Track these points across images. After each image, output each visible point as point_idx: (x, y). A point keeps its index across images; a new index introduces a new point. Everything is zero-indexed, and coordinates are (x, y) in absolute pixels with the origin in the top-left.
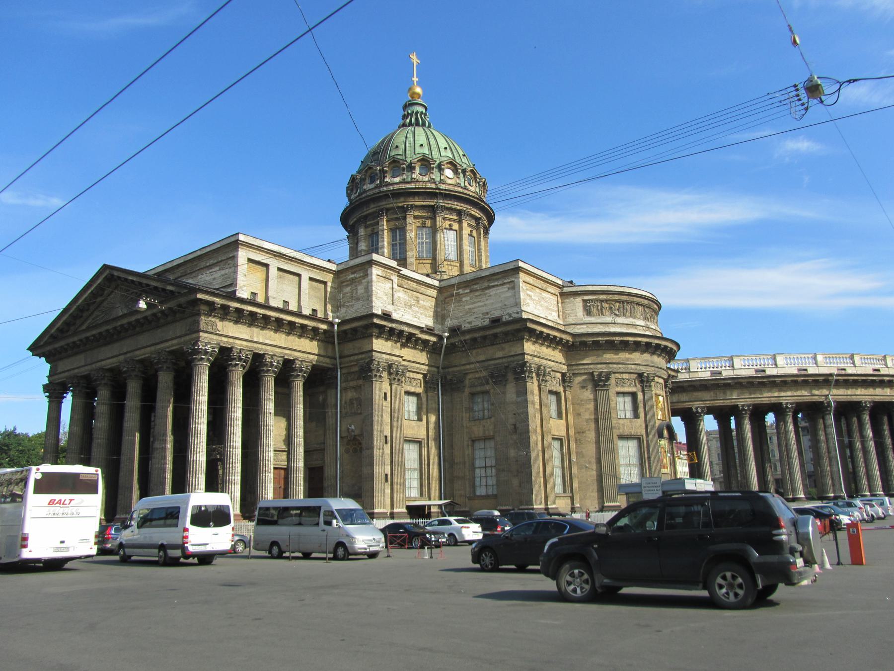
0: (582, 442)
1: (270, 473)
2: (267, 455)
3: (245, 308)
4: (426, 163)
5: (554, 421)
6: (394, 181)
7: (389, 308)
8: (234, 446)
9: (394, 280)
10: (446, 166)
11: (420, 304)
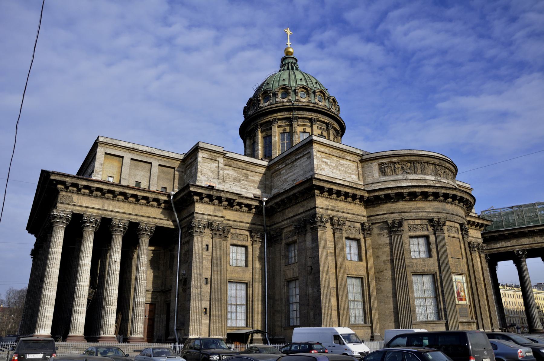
0: (380, 280)
1: (112, 305)
2: (110, 292)
3: (92, 185)
5: (352, 263)
6: (264, 105)
8: (81, 285)
9: (220, 161)
10: (300, 90)
11: (250, 179)
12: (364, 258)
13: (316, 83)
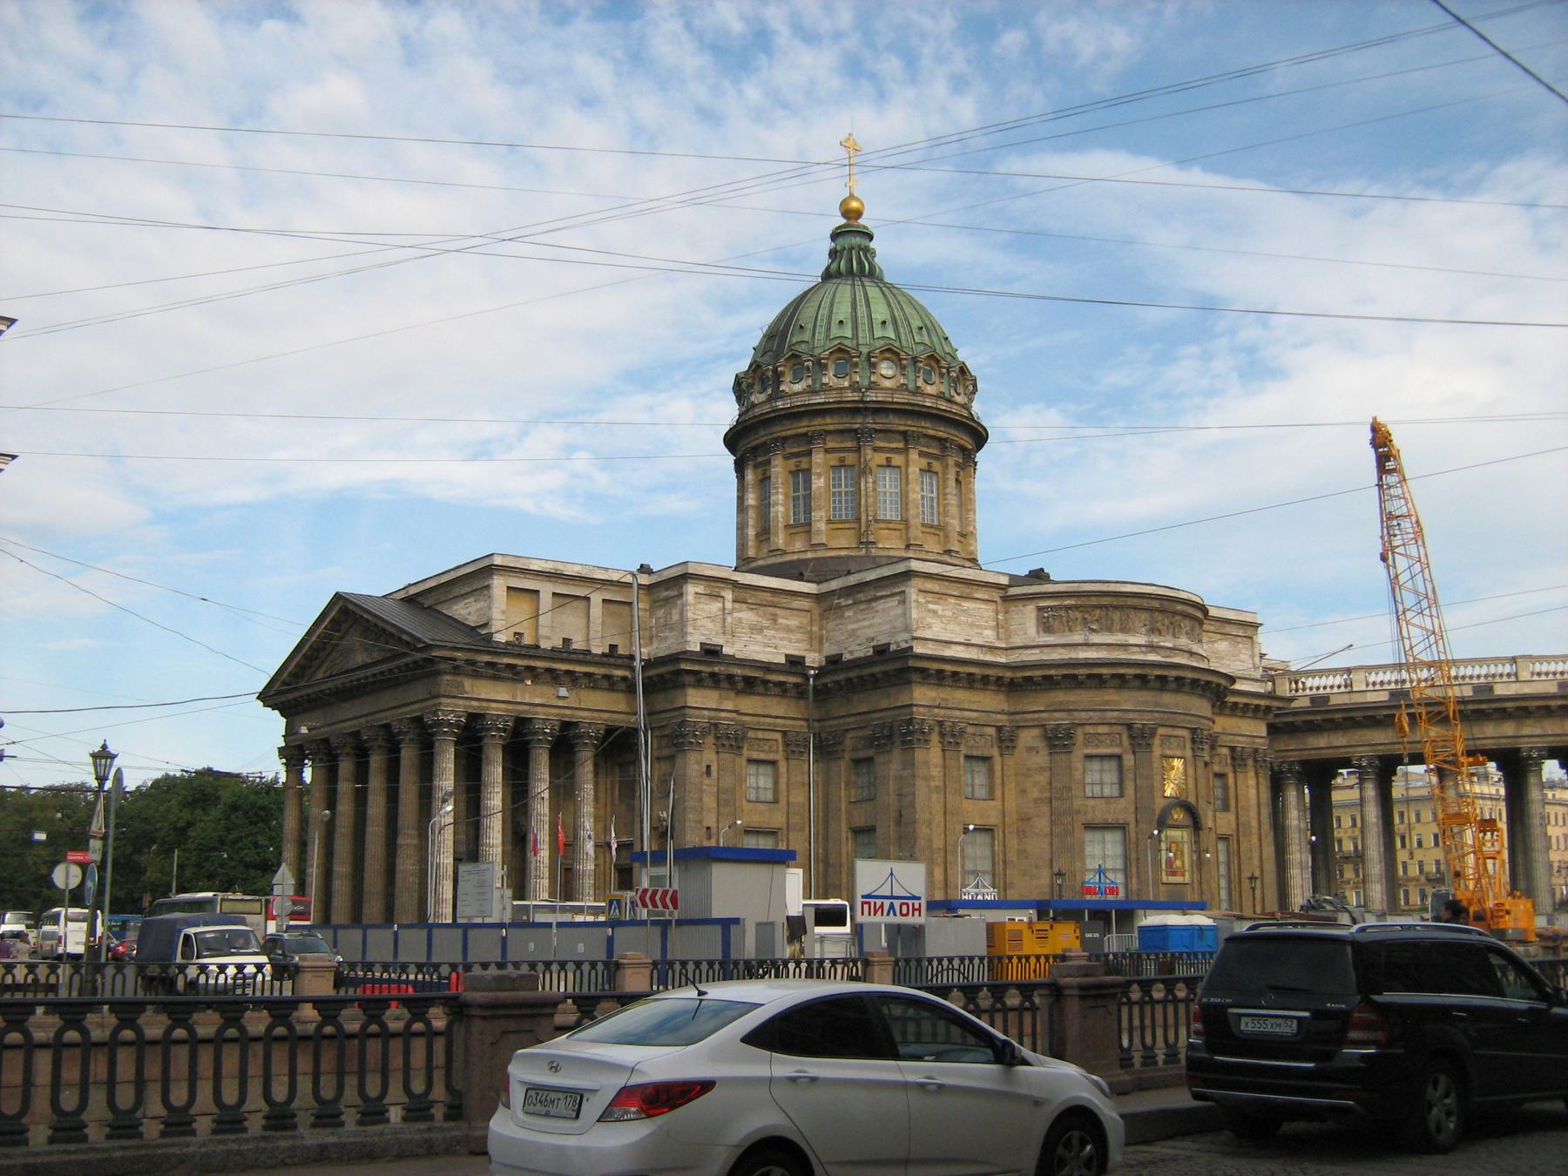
3: (500, 661)
4: (846, 356)
7: (717, 640)
12: (998, 793)
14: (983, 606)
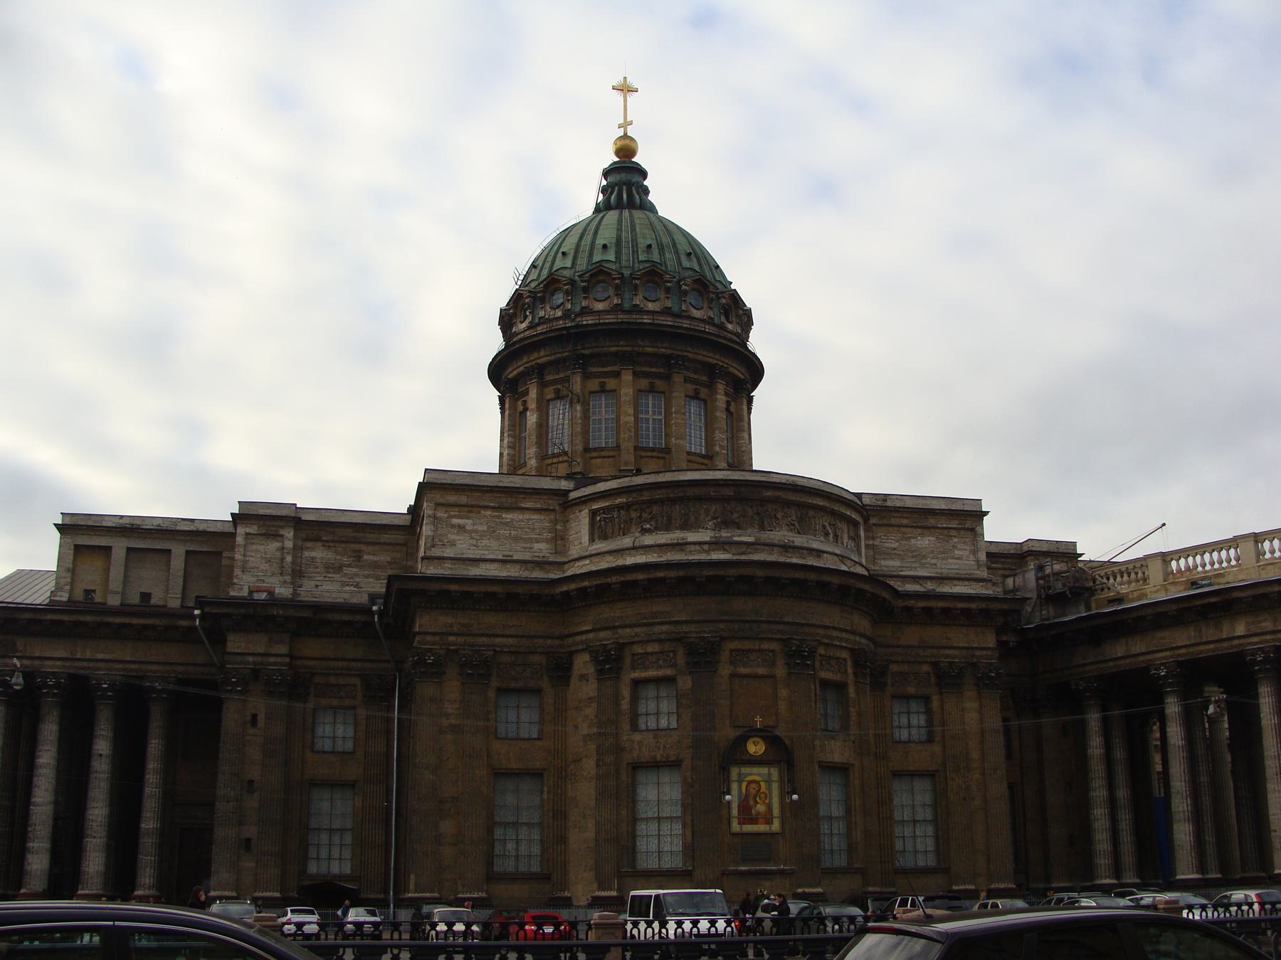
9: (286, 534)
11: (366, 560)
13: (649, 246)
14: (536, 517)
